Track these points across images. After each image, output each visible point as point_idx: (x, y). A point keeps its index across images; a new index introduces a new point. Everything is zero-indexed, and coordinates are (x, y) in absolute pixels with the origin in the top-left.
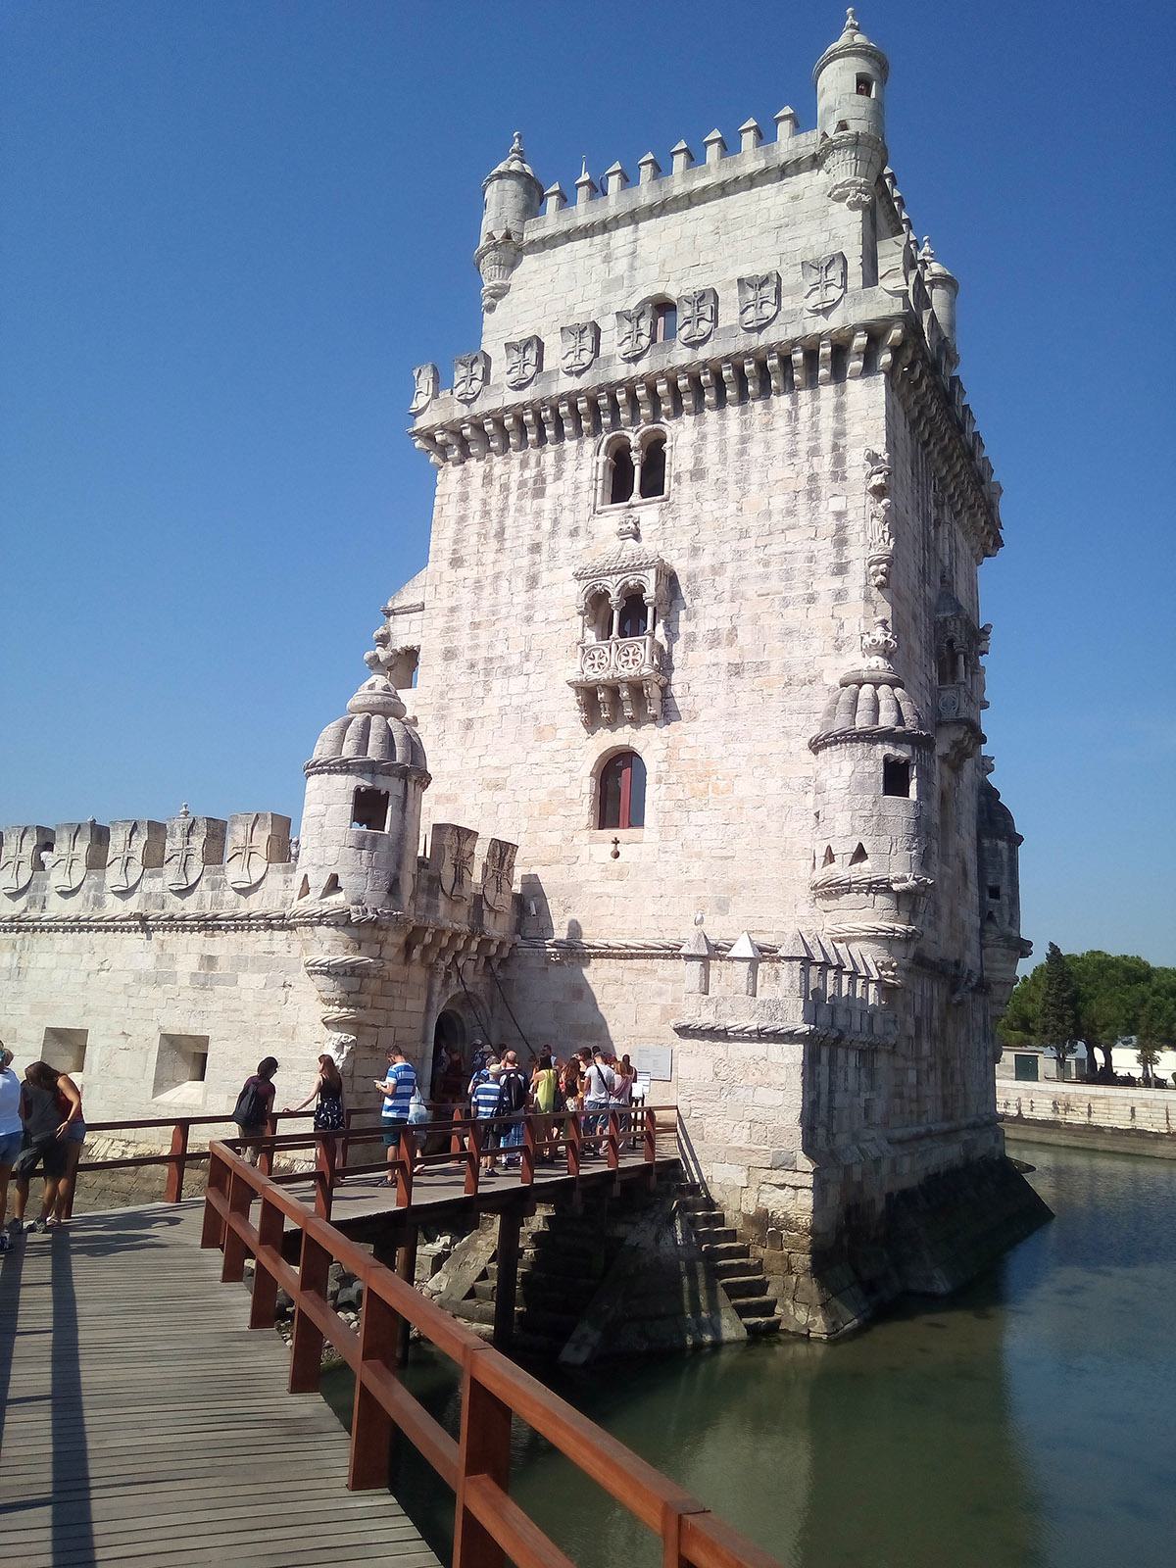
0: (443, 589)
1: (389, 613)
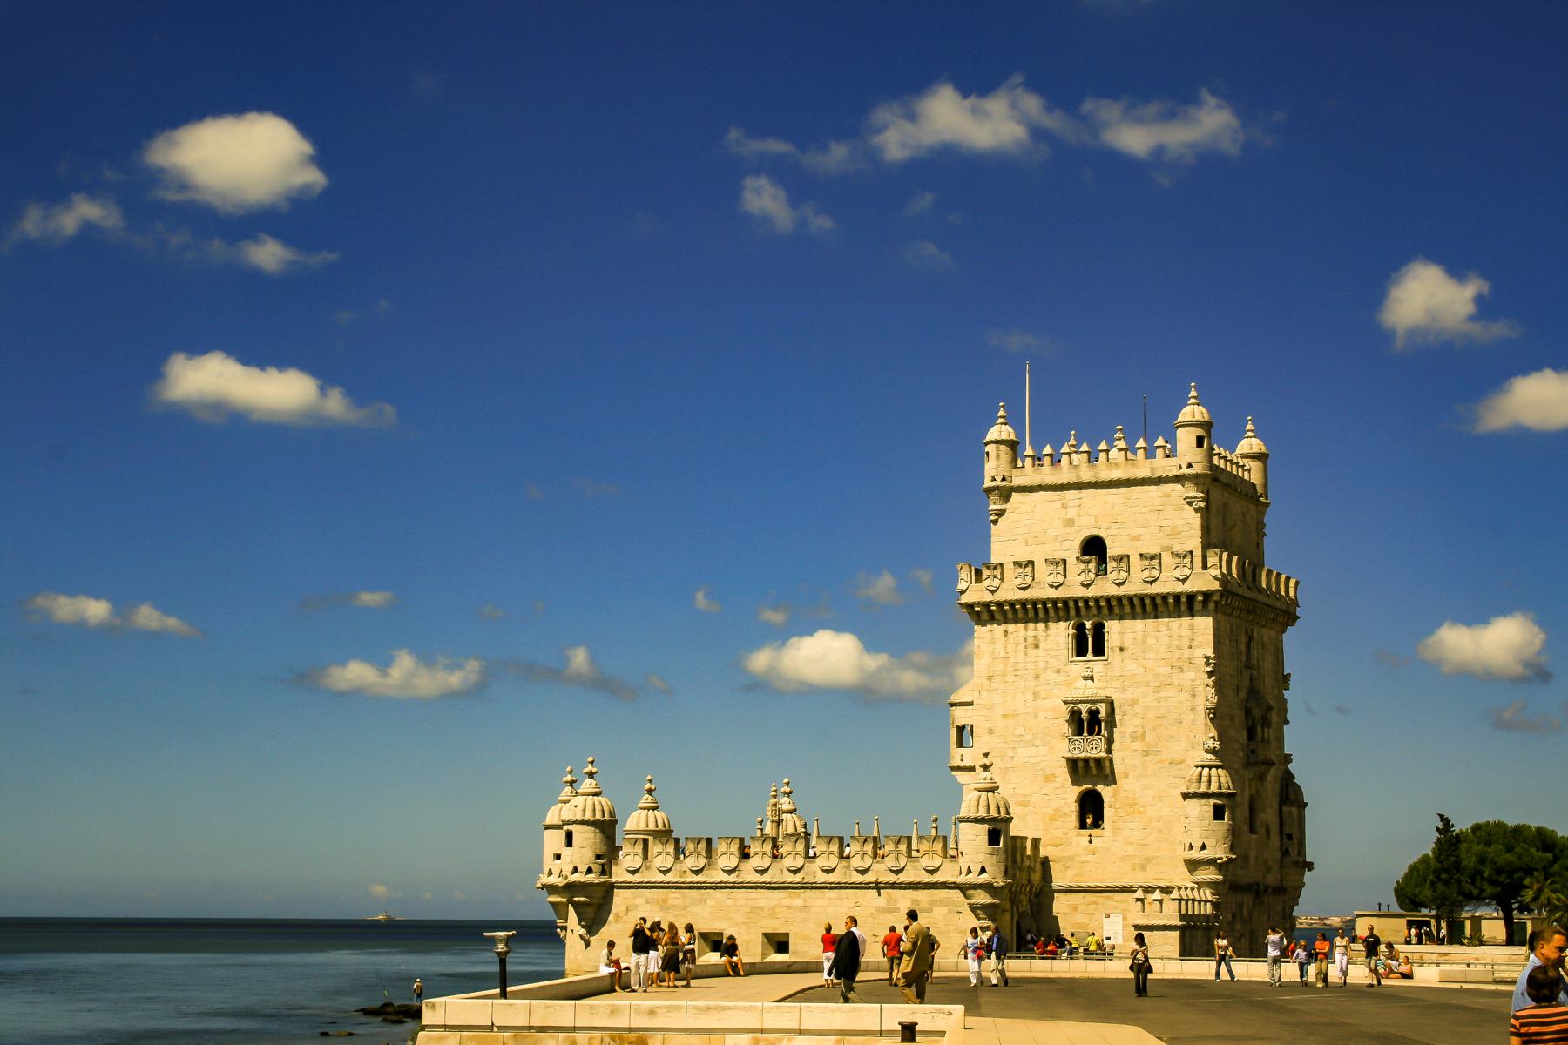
0: (985, 694)
1: (952, 705)
